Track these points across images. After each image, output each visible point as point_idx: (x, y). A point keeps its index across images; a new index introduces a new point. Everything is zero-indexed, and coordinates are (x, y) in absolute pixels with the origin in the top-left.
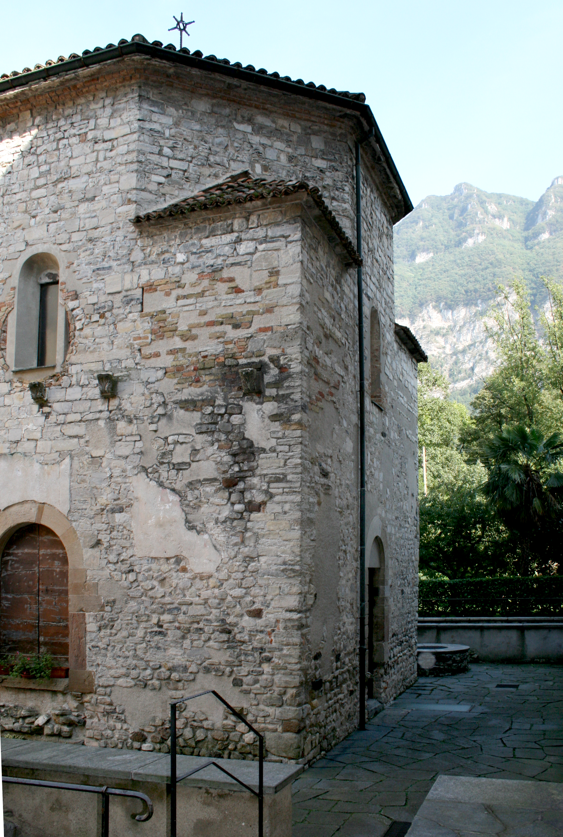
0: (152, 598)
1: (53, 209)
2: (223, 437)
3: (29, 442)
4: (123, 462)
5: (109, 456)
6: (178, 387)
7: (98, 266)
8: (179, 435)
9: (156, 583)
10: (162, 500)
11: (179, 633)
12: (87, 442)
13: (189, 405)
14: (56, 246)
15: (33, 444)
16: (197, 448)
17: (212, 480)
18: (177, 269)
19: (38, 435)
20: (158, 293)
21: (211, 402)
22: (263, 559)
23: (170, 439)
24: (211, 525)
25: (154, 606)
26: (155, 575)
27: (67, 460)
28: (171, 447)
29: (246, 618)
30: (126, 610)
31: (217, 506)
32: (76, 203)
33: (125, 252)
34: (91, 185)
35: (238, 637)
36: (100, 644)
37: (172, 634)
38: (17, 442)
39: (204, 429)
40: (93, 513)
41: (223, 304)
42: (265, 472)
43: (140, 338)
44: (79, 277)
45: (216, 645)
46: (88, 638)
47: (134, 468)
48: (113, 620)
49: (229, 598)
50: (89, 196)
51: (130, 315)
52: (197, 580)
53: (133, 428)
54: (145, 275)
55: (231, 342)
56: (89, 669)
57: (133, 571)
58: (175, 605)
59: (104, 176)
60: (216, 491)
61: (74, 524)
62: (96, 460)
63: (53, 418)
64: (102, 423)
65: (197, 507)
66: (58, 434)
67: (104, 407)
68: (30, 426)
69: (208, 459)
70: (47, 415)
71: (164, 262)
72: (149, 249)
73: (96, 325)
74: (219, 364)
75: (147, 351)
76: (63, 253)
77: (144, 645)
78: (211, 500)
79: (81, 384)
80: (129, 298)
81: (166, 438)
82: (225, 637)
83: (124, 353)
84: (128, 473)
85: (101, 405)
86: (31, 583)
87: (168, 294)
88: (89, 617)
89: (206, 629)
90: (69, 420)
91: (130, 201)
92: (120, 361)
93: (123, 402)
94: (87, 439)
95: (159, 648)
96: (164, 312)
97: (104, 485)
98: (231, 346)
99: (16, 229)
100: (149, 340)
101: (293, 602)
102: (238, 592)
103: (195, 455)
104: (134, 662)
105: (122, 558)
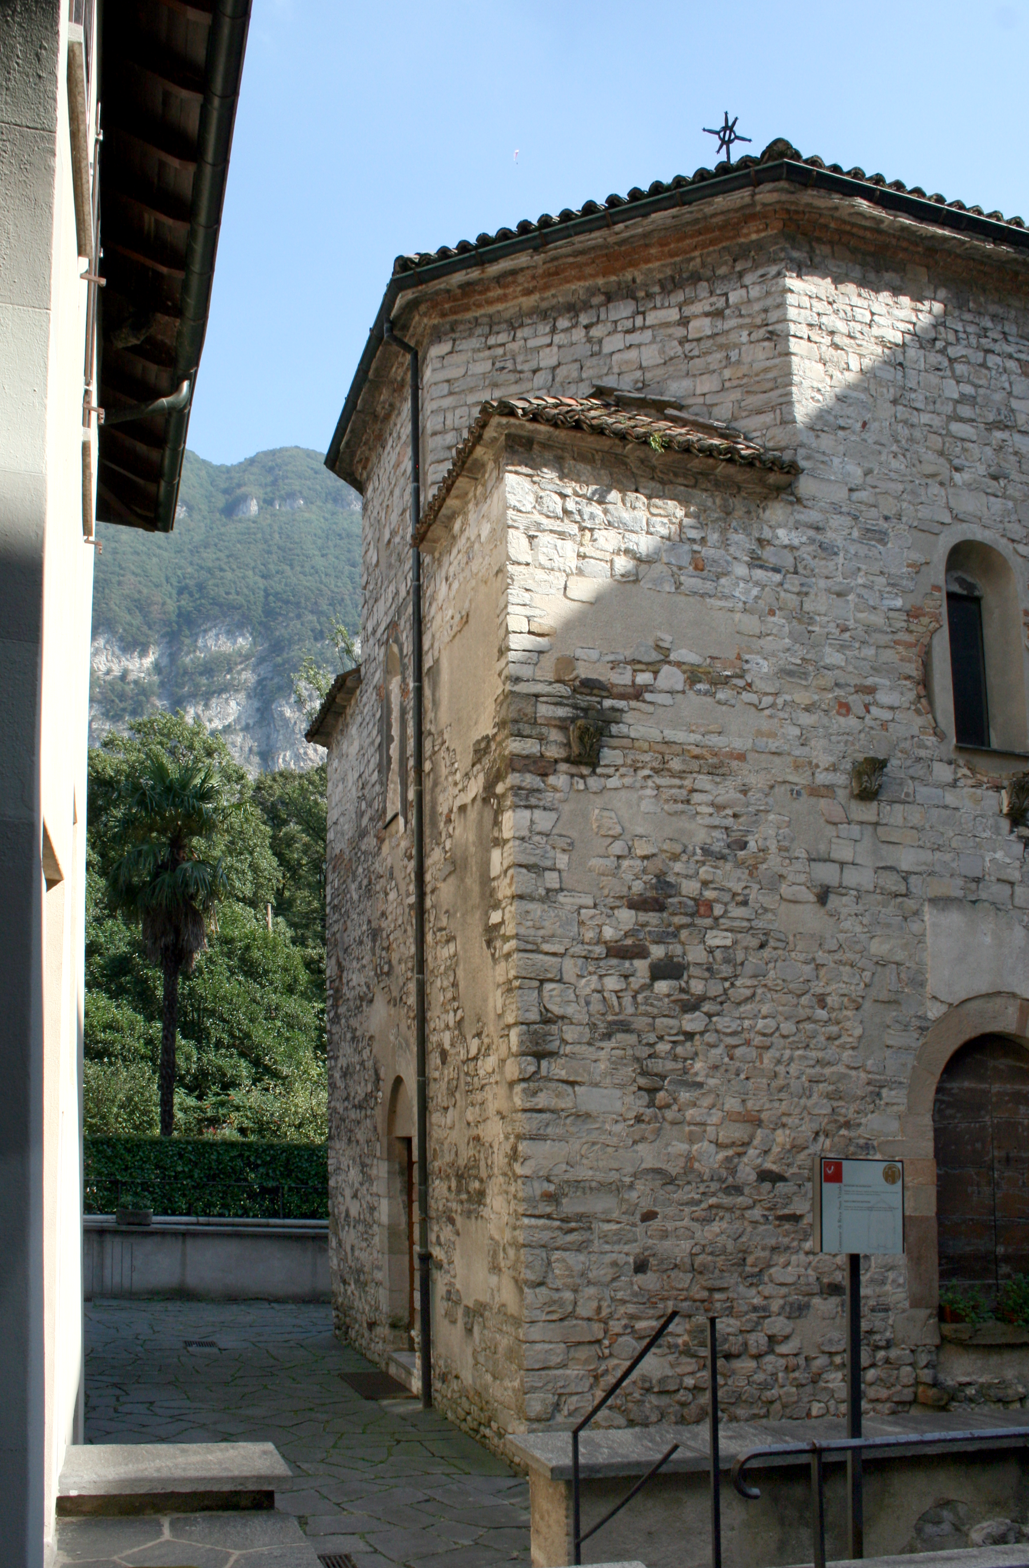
3: (1000, 886)
14: (1004, 541)
15: (1007, 889)
19: (1016, 875)
38: (977, 880)
68: (999, 855)
76: (1020, 560)
86: (978, 1145)
99: (928, 476)
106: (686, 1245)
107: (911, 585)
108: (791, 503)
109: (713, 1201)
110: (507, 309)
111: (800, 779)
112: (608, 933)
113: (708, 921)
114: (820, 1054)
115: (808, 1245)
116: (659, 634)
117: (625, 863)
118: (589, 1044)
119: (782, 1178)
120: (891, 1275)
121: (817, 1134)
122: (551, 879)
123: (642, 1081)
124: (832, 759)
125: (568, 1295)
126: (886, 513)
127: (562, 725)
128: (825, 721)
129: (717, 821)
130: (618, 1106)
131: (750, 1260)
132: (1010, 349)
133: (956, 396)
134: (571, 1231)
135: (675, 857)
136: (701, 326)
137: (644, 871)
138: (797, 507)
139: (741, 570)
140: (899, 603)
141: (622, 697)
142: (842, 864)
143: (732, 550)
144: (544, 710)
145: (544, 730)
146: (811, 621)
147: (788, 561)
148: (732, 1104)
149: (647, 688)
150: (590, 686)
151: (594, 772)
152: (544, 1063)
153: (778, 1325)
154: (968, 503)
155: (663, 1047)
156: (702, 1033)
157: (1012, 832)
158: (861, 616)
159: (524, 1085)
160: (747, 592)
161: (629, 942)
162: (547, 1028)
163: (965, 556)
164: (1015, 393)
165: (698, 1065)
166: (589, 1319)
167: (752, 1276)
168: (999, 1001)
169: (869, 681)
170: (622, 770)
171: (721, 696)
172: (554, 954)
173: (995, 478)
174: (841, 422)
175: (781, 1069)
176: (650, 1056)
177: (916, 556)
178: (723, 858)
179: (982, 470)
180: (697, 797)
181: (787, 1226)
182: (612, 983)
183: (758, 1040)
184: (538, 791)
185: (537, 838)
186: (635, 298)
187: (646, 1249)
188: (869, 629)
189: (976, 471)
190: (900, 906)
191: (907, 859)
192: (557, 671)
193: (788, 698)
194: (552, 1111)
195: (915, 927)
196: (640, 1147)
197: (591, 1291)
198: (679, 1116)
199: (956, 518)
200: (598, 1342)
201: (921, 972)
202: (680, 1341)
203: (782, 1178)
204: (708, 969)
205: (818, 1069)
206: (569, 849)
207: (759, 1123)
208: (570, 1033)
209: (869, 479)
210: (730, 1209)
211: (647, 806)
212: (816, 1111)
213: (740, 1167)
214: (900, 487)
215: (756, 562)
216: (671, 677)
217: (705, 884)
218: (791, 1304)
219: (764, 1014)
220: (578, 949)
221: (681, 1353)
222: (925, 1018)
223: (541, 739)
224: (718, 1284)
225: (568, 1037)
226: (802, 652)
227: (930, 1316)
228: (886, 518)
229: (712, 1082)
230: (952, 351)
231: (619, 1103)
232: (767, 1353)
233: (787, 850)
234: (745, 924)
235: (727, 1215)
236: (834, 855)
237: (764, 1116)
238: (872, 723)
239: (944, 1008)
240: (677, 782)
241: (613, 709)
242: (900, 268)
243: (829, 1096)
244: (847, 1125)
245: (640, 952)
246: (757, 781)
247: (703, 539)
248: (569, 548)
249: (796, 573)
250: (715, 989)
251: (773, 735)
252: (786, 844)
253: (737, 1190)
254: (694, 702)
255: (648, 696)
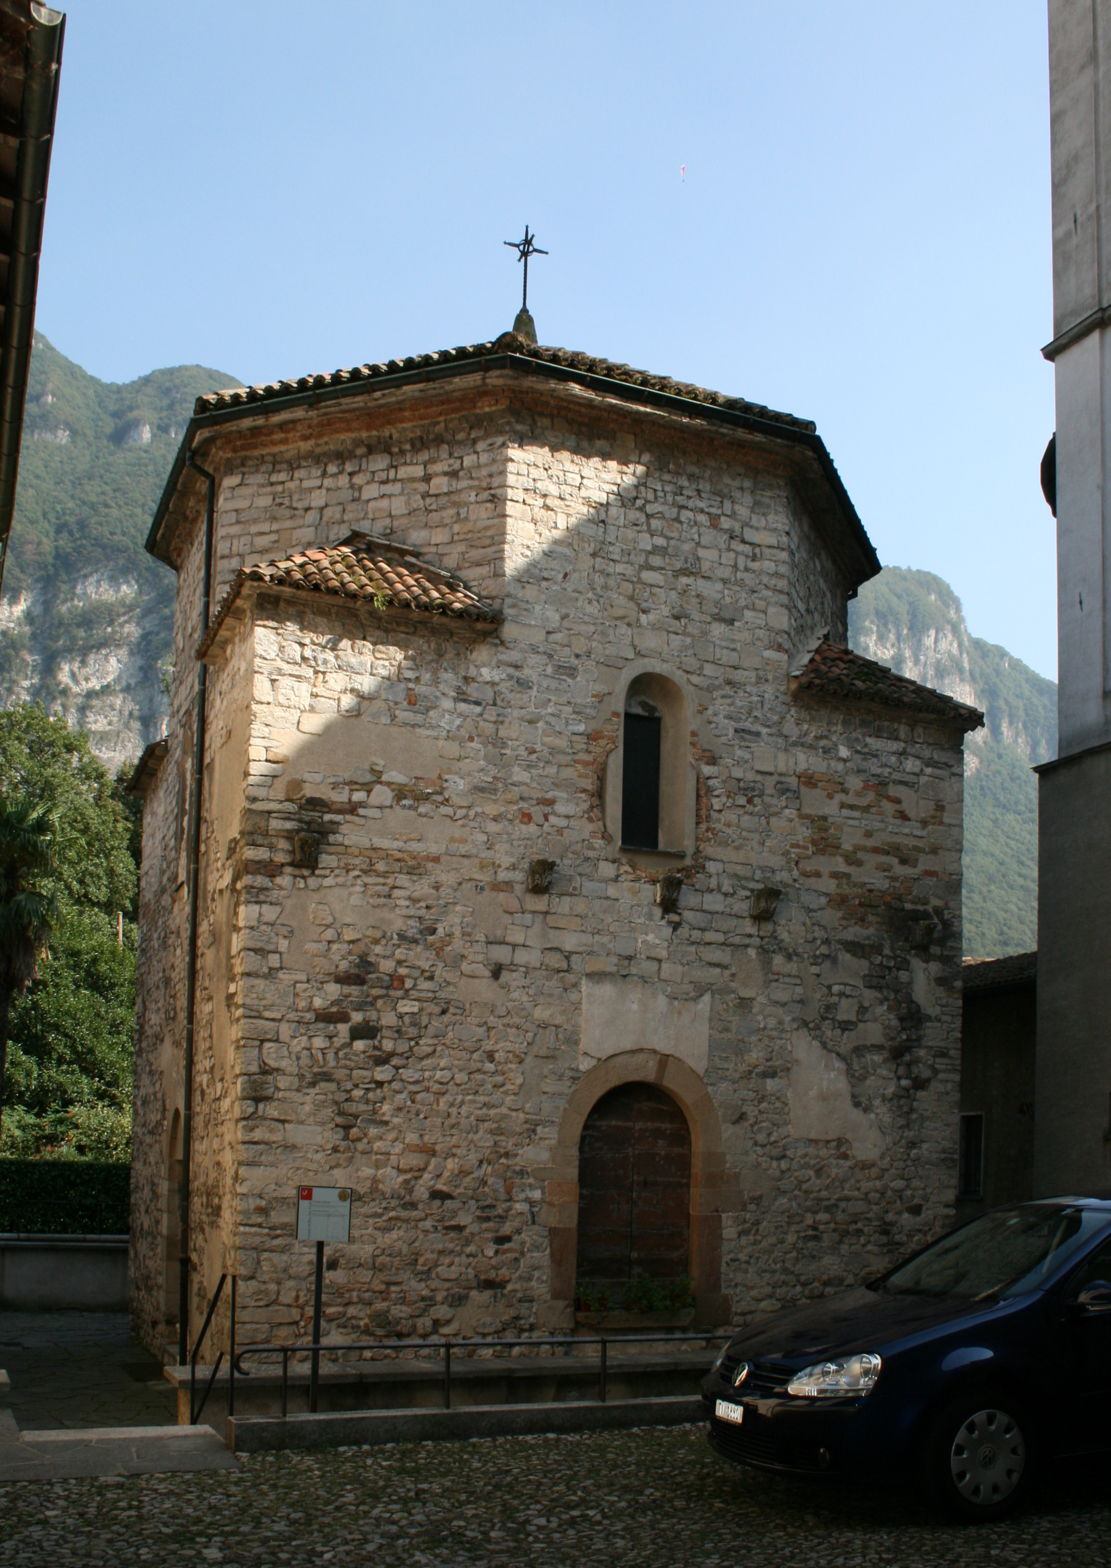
0: (806, 1192)
1: (675, 611)
2: (892, 996)
3: (649, 962)
4: (780, 1011)
5: (761, 999)
6: (844, 922)
7: (741, 725)
8: (845, 985)
9: (811, 1173)
10: (826, 1066)
11: (836, 1236)
12: (733, 975)
13: (855, 948)
14: (680, 672)
15: (655, 965)
16: (866, 1005)
17: (880, 1048)
18: (840, 766)
19: (664, 954)
20: (818, 791)
21: (878, 949)
22: (925, 1146)
23: (836, 989)
24: (877, 1102)
25: (809, 1203)
26: (812, 1162)
27: (707, 998)
28: (834, 999)
29: (906, 1215)
30: (773, 1208)
31: (883, 1080)
32: (709, 619)
33: (776, 718)
34: (728, 600)
35: (897, 1238)
36: (740, 1256)
37: (827, 1240)
38: (630, 958)
39: (875, 981)
40: (737, 1075)
41: (890, 828)
42: (930, 1044)
43: (798, 846)
44: (716, 732)
45: (876, 1249)
46: (725, 1248)
47: (794, 1020)
48: (757, 1223)
49: (889, 1192)
50: (727, 615)
51: (787, 811)
52: (857, 1170)
53: (792, 967)
54: (803, 760)
55: (894, 879)
56: (724, 1291)
57: (784, 1156)
58: (832, 1202)
59: (744, 595)
60: (885, 1061)
61: (710, 1089)
62: (745, 1004)
63: (684, 931)
64: (752, 952)
65: (863, 1078)
66: (693, 957)
67: (753, 931)
68: (650, 937)
69: (875, 1020)
70: (676, 926)
71: (826, 751)
72: (805, 727)
73: (741, 811)
74: (885, 904)
75: (809, 867)
76: (692, 688)
77: (794, 1254)
78: (879, 1071)
79: (724, 890)
80: (784, 786)
81: (829, 987)
82: (884, 1239)
83: (777, 861)
84: (787, 1027)
85: (749, 927)
87: (830, 796)
88: (727, 1219)
89: (866, 1229)
90: (707, 940)
91: (780, 648)
92: (773, 871)
93: (779, 928)
94: (733, 970)
95: (813, 1257)
96: (824, 818)
97: (754, 1038)
98: (897, 885)
99: (617, 619)
100: (810, 852)
101: (950, 1195)
102: (899, 1184)
103: (864, 1013)
104: (783, 1277)
105: (772, 1139)
106: (369, 1249)
107: (593, 712)
108: (496, 645)
109: (392, 1214)
110: (289, 450)
111: (485, 877)
112: (318, 1002)
113: (400, 993)
114: (487, 1099)
115: (468, 1250)
116: (375, 759)
117: (335, 947)
118: (298, 1090)
119: (449, 1196)
120: (536, 1274)
121: (481, 1162)
122: (274, 960)
123: (339, 1120)
124: (512, 860)
125: (273, 1287)
126: (577, 651)
127: (289, 836)
128: (509, 828)
129: (412, 912)
130: (319, 1139)
131: (421, 1260)
132: (702, 505)
133: (649, 548)
134: (277, 1236)
135: (376, 942)
136: (440, 484)
137: (350, 953)
138: (501, 649)
139: (447, 704)
140: (581, 728)
141: (340, 812)
142: (514, 946)
143: (441, 687)
144: (275, 824)
145: (274, 840)
146: (504, 745)
147: (489, 694)
148: (412, 1138)
149: (361, 804)
150: (314, 803)
151: (313, 874)
152: (261, 1106)
153: (441, 1311)
154: (651, 641)
155: (357, 1093)
156: (390, 1082)
157: (663, 918)
158: (546, 739)
159: (244, 1123)
160: (451, 722)
161: (334, 1009)
162: (264, 1078)
163: (644, 685)
164: (703, 543)
165: (386, 1108)
166: (289, 1306)
167: (422, 1273)
168: (641, 1057)
169: (549, 795)
170: (337, 871)
171: (422, 810)
172: (273, 1020)
173: (677, 618)
174: (545, 574)
175: (453, 1111)
176: (347, 1100)
177: (601, 688)
178: (415, 941)
179: (665, 611)
180: (397, 893)
181: (452, 1234)
182: (319, 1042)
183: (436, 1087)
184: (267, 889)
185: (264, 927)
186: (391, 454)
187: (337, 1251)
188: (553, 750)
189: (661, 612)
190: (562, 979)
191: (570, 941)
192: (287, 792)
193: (479, 810)
194: (266, 1143)
195: (574, 996)
196: (335, 1172)
197: (291, 1283)
198: (368, 1148)
199: (639, 654)
200: (296, 1323)
201: (575, 1032)
202: (362, 1323)
203: (449, 1196)
204: (398, 1031)
205: (484, 1110)
206: (290, 935)
207: (433, 1153)
208: (283, 1082)
209: (565, 623)
210: (407, 1221)
211: (355, 900)
212: (481, 1144)
213: (417, 1188)
214: (592, 628)
215: (461, 697)
216: (382, 795)
217: (400, 963)
218: (453, 1296)
219: (442, 1067)
220: (292, 1016)
221: (362, 1332)
222: (577, 1070)
223: (272, 847)
224: (394, 1279)
225: (281, 1085)
226: (494, 771)
227: (567, 1306)
228: (577, 656)
229: (396, 1120)
230: (649, 509)
231: (319, 1138)
232: (431, 1334)
233: (469, 935)
234: (430, 995)
235: (404, 1226)
236: (508, 939)
237: (438, 1148)
238: (550, 830)
239: (594, 1062)
240: (381, 880)
241: (332, 822)
242: (611, 437)
243: (492, 1132)
244: (507, 1155)
245: (344, 1018)
246: (448, 879)
247: (417, 679)
248: (304, 688)
249: (495, 704)
250: (403, 1046)
251: (464, 841)
252: (469, 930)
253: (413, 1205)
254: (399, 815)
255: (361, 811)
